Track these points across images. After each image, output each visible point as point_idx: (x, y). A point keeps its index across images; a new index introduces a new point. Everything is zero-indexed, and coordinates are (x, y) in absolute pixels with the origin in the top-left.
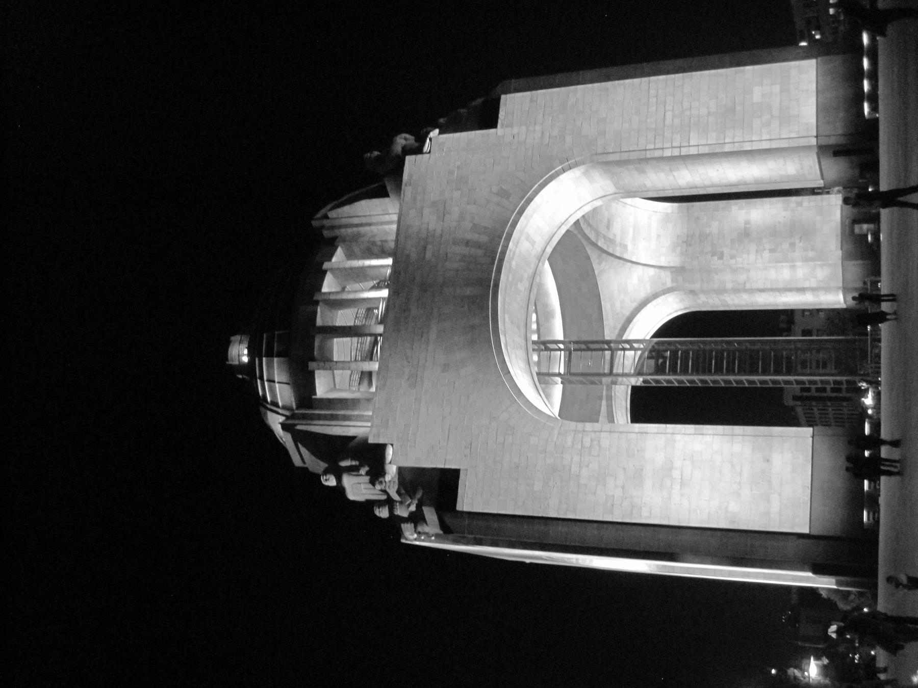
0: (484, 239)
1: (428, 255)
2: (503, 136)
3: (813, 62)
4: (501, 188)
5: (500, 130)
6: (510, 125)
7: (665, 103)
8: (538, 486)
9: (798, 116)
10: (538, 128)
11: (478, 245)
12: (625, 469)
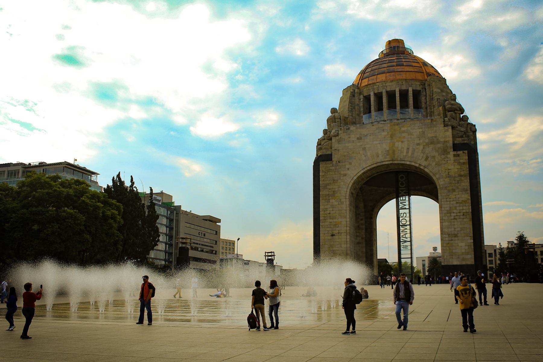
0: (410, 154)
1: (404, 135)
2: (450, 154)
3: (473, 263)
4: (429, 158)
5: (452, 153)
6: (454, 155)
7: (460, 212)
8: (328, 187)
9: (453, 258)
10: (452, 167)
11: (407, 152)
12: (335, 213)
